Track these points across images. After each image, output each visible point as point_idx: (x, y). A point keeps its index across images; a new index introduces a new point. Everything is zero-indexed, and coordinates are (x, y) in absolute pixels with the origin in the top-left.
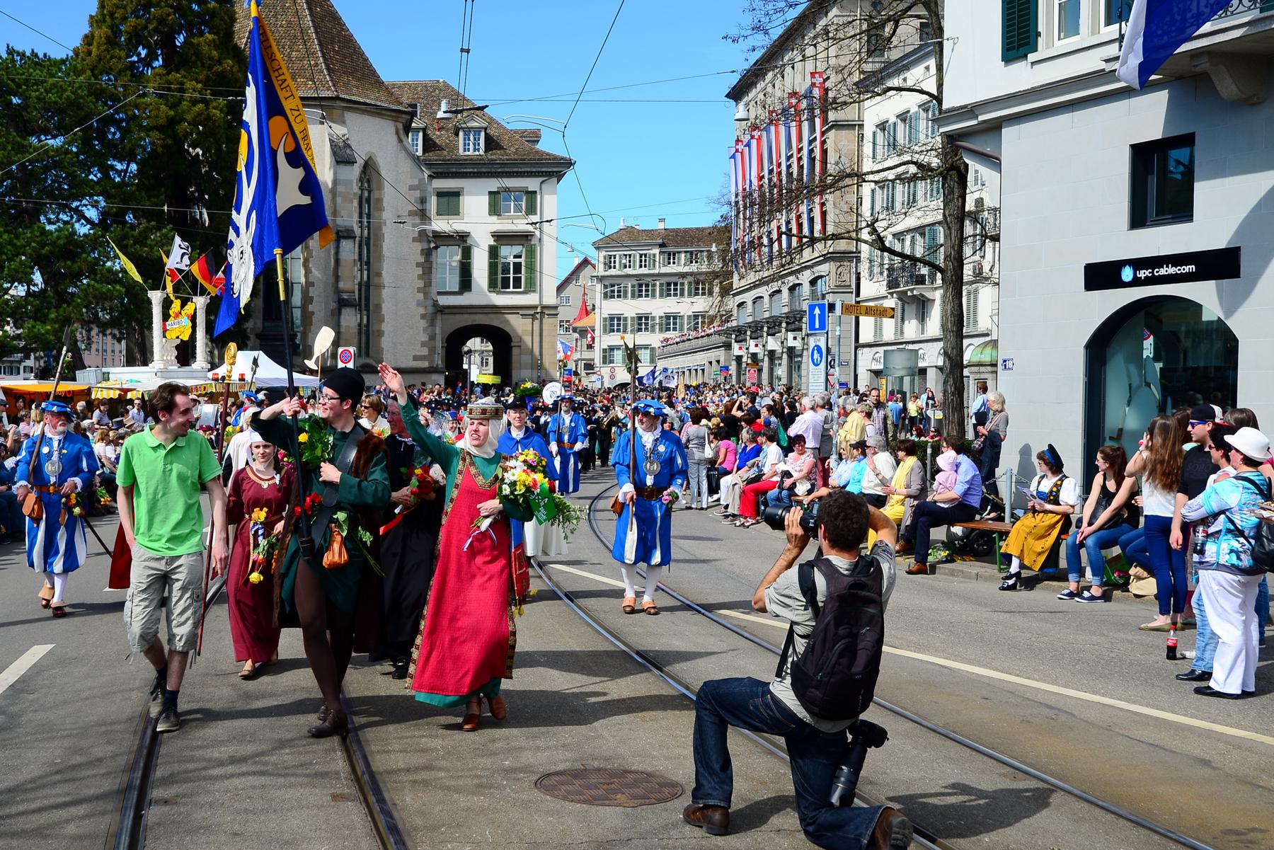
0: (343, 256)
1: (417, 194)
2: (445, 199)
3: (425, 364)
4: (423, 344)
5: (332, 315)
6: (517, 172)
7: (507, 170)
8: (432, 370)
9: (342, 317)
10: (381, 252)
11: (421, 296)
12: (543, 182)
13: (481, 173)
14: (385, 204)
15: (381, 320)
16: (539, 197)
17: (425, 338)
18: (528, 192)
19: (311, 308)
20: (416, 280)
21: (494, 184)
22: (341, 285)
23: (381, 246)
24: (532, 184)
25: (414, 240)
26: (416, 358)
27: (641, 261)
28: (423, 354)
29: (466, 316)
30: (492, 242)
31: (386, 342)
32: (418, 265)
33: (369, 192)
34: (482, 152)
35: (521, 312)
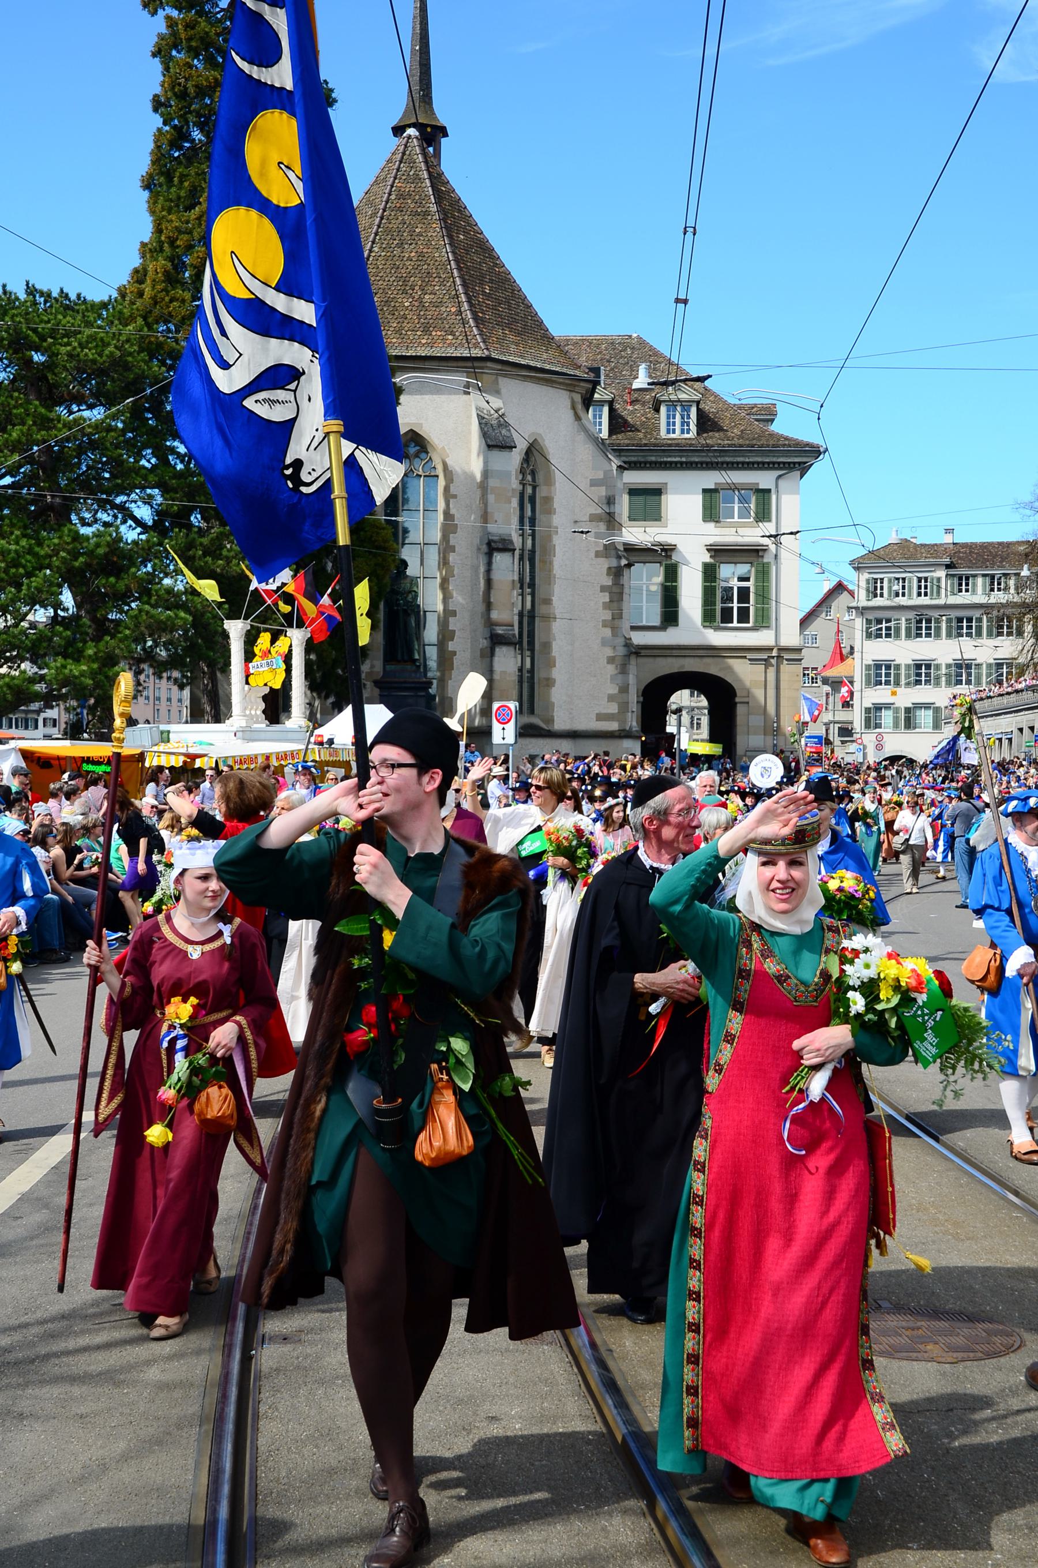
0: (496, 575)
1: (602, 491)
2: (640, 499)
3: (613, 726)
4: (611, 698)
5: (482, 656)
6: (743, 463)
7: (728, 459)
8: (624, 734)
9: (496, 659)
10: (550, 570)
11: (608, 632)
13: (691, 463)
14: (556, 505)
15: (551, 663)
16: (774, 497)
17: (614, 690)
18: (758, 491)
19: (451, 646)
21: (711, 479)
22: (495, 615)
23: (551, 563)
24: (765, 479)
25: (598, 555)
27: (920, 587)
29: (670, 660)
30: (707, 558)
31: (557, 695)
32: (603, 589)
33: (534, 488)
34: (693, 434)
35: (749, 656)
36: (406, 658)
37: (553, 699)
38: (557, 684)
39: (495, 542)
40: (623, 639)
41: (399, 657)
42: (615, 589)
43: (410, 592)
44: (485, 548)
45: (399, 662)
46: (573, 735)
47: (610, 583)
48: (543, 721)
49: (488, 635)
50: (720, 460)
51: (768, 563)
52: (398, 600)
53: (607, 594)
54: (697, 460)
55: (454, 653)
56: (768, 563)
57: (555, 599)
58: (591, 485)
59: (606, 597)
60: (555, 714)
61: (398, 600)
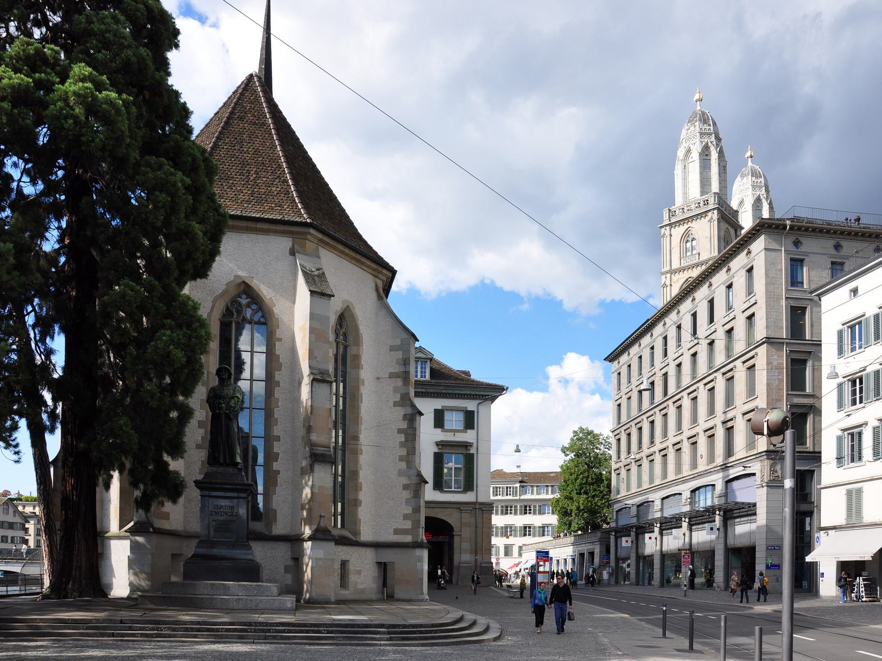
1: (400, 355)
3: (408, 539)
4: (406, 517)
8: (417, 545)
10: (358, 413)
11: (403, 465)
13: (428, 393)
14: (363, 362)
17: (408, 510)
19: (276, 466)
23: (358, 408)
24: (471, 405)
25: (396, 404)
26: (397, 532)
28: (406, 527)
32: (400, 431)
36: (228, 461)
41: (222, 461)
42: (410, 432)
43: (233, 398)
45: (221, 465)
46: (377, 546)
49: (308, 454)
50: (444, 392)
51: (473, 454)
52: (220, 403)
53: (403, 435)
55: (278, 472)
56: (473, 454)
57: (362, 437)
58: (391, 350)
59: (402, 438)
60: (361, 528)
61: (220, 403)
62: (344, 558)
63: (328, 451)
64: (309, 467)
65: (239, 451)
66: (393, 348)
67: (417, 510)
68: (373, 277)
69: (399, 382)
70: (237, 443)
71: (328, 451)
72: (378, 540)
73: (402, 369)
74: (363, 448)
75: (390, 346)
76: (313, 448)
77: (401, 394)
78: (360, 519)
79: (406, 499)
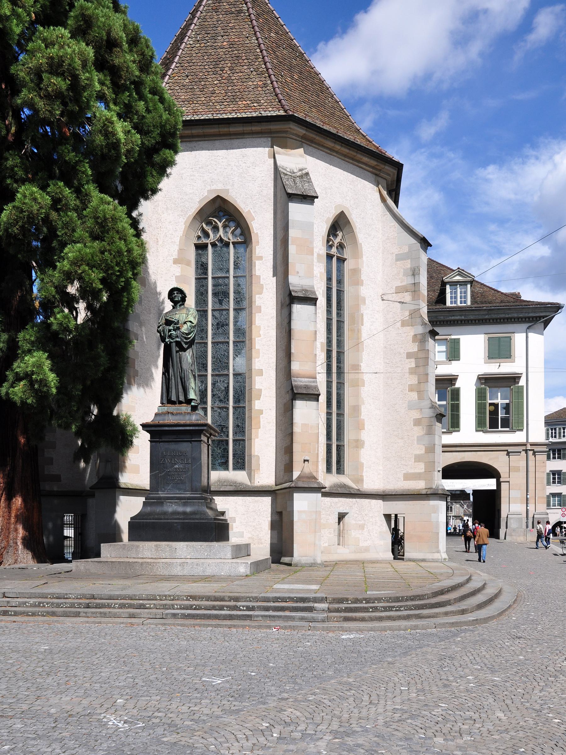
1: (408, 264)
4: (418, 459)
7: (494, 316)
11: (414, 395)
12: (530, 326)
14: (363, 277)
15: (360, 426)
17: (421, 450)
20: (407, 375)
22: (295, 367)
23: (359, 331)
25: (404, 324)
26: (408, 477)
32: (409, 355)
34: (469, 303)
37: (362, 460)
38: (367, 444)
39: (296, 292)
40: (429, 402)
41: (174, 398)
42: (421, 355)
43: (185, 323)
44: (288, 301)
45: (173, 403)
47: (416, 349)
48: (353, 481)
50: (486, 317)
52: (170, 331)
53: (413, 360)
54: (472, 318)
58: (397, 260)
60: (364, 474)
62: (342, 510)
63: (314, 382)
64: (290, 401)
65: (194, 387)
66: (399, 258)
67: (431, 449)
68: (374, 176)
69: (407, 297)
70: (191, 376)
71: (314, 382)
72: (385, 489)
73: (410, 280)
74: (366, 377)
75: (396, 255)
76: (295, 379)
77: (410, 311)
78: (363, 464)
79: (417, 437)
